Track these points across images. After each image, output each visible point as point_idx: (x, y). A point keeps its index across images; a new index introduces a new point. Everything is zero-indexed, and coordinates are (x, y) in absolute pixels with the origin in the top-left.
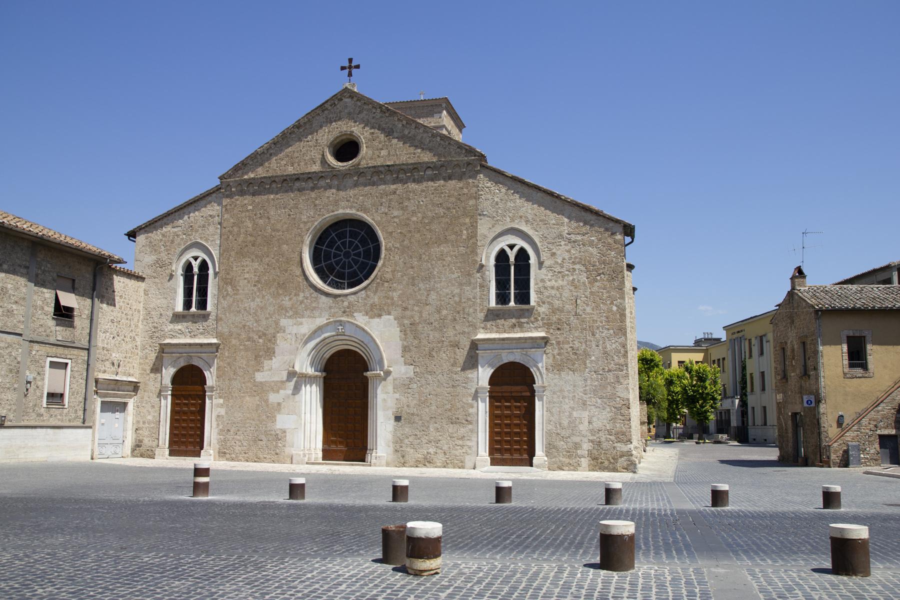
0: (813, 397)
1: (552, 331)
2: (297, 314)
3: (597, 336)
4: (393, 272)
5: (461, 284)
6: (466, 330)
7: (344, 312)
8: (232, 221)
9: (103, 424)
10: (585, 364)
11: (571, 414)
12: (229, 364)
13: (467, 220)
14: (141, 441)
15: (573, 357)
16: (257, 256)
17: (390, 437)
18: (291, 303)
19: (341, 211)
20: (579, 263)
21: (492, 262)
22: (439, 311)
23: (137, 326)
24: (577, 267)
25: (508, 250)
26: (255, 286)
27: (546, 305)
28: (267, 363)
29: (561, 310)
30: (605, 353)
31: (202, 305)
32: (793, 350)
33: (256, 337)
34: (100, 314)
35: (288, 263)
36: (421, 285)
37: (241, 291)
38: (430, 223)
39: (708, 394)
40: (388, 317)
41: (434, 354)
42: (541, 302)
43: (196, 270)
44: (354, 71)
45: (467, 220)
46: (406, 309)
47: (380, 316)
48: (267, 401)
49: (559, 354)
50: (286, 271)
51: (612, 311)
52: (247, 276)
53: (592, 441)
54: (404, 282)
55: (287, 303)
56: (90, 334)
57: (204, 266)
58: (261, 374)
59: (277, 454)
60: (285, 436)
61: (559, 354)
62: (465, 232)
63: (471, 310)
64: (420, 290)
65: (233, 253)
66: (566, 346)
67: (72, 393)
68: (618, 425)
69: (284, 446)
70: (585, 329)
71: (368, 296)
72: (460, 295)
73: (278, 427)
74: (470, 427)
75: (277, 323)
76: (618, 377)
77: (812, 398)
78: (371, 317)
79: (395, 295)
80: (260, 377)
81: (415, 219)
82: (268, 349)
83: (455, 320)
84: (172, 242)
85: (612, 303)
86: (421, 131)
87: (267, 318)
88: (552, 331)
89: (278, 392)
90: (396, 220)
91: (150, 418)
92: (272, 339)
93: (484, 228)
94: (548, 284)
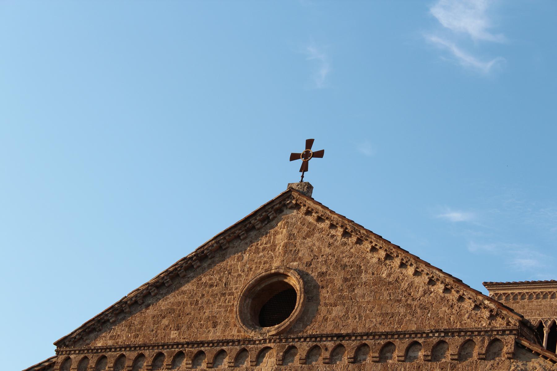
44: (313, 162)
86: (410, 271)
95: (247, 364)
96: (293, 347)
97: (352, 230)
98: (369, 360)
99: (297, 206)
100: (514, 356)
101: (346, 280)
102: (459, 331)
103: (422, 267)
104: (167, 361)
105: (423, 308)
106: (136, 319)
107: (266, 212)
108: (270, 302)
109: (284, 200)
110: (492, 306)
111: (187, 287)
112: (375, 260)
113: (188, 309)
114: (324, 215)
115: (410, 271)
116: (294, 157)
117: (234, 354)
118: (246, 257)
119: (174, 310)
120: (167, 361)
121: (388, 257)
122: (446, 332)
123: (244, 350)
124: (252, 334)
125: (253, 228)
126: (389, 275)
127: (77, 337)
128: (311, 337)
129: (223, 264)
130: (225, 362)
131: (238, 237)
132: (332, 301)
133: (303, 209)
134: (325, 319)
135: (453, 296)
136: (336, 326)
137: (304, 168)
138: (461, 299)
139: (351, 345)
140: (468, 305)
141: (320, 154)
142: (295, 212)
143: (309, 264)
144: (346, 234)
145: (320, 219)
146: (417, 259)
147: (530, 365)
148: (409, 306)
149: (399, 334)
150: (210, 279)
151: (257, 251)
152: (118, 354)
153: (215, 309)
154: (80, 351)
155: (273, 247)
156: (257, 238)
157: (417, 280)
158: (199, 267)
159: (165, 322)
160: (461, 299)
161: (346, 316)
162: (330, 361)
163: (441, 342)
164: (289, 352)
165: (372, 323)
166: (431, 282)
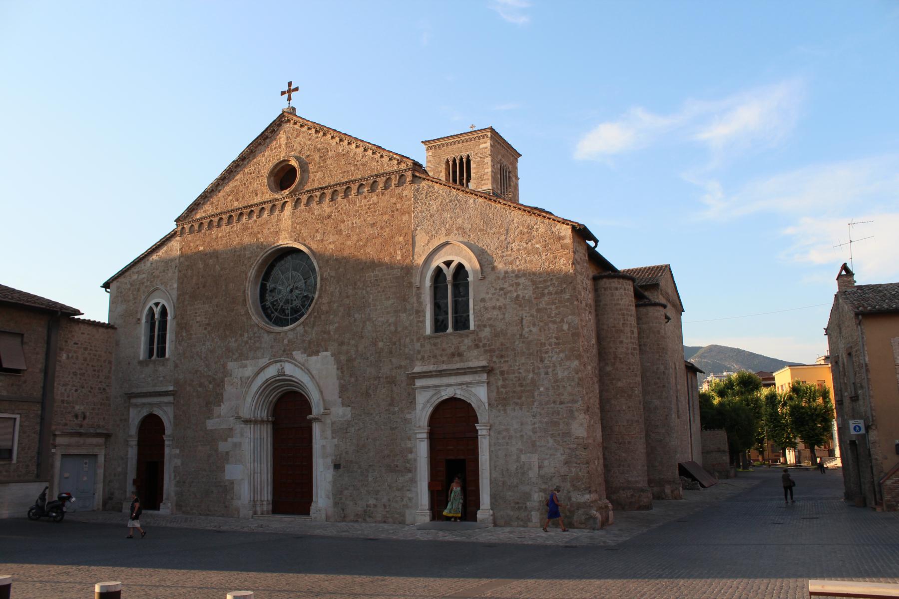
0: (862, 422)
1: (495, 359)
2: (242, 357)
3: (546, 362)
4: (329, 303)
5: (396, 312)
6: (403, 364)
7: (284, 351)
8: (186, 263)
9: (67, 478)
10: (534, 398)
11: (518, 458)
13: (401, 239)
14: (112, 494)
15: (519, 389)
17: (329, 487)
21: (428, 283)
22: (375, 344)
23: (108, 377)
24: (522, 280)
25: (443, 266)
26: (205, 329)
27: (487, 329)
28: (216, 410)
30: (556, 381)
31: (162, 352)
32: (843, 364)
33: (207, 383)
34: (58, 368)
36: (356, 316)
37: (194, 336)
38: (364, 246)
39: (817, 415)
40: (325, 353)
41: (370, 391)
42: (481, 327)
43: (156, 316)
45: (401, 239)
46: (342, 344)
47: (317, 353)
50: (232, 311)
52: (198, 319)
53: (544, 491)
54: (340, 314)
55: (233, 345)
56: (44, 388)
57: (164, 312)
58: (211, 421)
59: (226, 507)
60: (233, 488)
61: (504, 386)
62: (399, 252)
63: (408, 340)
64: (355, 320)
65: (187, 297)
66: (512, 376)
67: (21, 448)
68: (574, 470)
69: (232, 499)
70: (531, 354)
71: (305, 331)
73: (227, 478)
74: (410, 475)
75: (224, 366)
76: (571, 411)
77: (861, 423)
78: (309, 355)
79: (332, 328)
80: (211, 424)
81: (349, 243)
83: (391, 352)
84: (139, 290)
86: (354, 146)
87: (216, 363)
88: (495, 359)
89: (226, 440)
90: (331, 246)
91: (119, 470)
92: (220, 384)
94: (488, 304)
95: (277, 212)
96: (299, 199)
97: (319, 129)
98: (339, 198)
99: (289, 121)
100: (412, 182)
101: (321, 157)
102: (383, 174)
103: (359, 143)
104: (235, 219)
105: (363, 165)
106: (215, 199)
108: (284, 176)
110: (398, 157)
111: (238, 177)
112: (334, 143)
113: (241, 188)
114: (304, 123)
115: (354, 146)
116: (283, 93)
117: (269, 208)
118: (266, 154)
120: (235, 219)
121: (341, 140)
122: (376, 176)
123: (274, 205)
124: (277, 196)
128: (307, 191)
129: (255, 161)
130: (266, 214)
133: (292, 122)
134: (314, 180)
135: (378, 156)
136: (320, 183)
137: (289, 99)
138: (382, 156)
139: (329, 192)
140: (386, 159)
141: (296, 89)
142: (288, 125)
143: (300, 152)
144: (317, 132)
145: (302, 126)
146: (356, 139)
147: (421, 185)
149: (352, 181)
151: (272, 150)
152: (208, 220)
153: (255, 186)
155: (280, 147)
156: (270, 143)
157: (358, 150)
159: (230, 198)
160: (382, 156)
161: (324, 177)
162: (320, 202)
163: (375, 182)
164: (298, 202)
165: (339, 178)
166: (365, 150)
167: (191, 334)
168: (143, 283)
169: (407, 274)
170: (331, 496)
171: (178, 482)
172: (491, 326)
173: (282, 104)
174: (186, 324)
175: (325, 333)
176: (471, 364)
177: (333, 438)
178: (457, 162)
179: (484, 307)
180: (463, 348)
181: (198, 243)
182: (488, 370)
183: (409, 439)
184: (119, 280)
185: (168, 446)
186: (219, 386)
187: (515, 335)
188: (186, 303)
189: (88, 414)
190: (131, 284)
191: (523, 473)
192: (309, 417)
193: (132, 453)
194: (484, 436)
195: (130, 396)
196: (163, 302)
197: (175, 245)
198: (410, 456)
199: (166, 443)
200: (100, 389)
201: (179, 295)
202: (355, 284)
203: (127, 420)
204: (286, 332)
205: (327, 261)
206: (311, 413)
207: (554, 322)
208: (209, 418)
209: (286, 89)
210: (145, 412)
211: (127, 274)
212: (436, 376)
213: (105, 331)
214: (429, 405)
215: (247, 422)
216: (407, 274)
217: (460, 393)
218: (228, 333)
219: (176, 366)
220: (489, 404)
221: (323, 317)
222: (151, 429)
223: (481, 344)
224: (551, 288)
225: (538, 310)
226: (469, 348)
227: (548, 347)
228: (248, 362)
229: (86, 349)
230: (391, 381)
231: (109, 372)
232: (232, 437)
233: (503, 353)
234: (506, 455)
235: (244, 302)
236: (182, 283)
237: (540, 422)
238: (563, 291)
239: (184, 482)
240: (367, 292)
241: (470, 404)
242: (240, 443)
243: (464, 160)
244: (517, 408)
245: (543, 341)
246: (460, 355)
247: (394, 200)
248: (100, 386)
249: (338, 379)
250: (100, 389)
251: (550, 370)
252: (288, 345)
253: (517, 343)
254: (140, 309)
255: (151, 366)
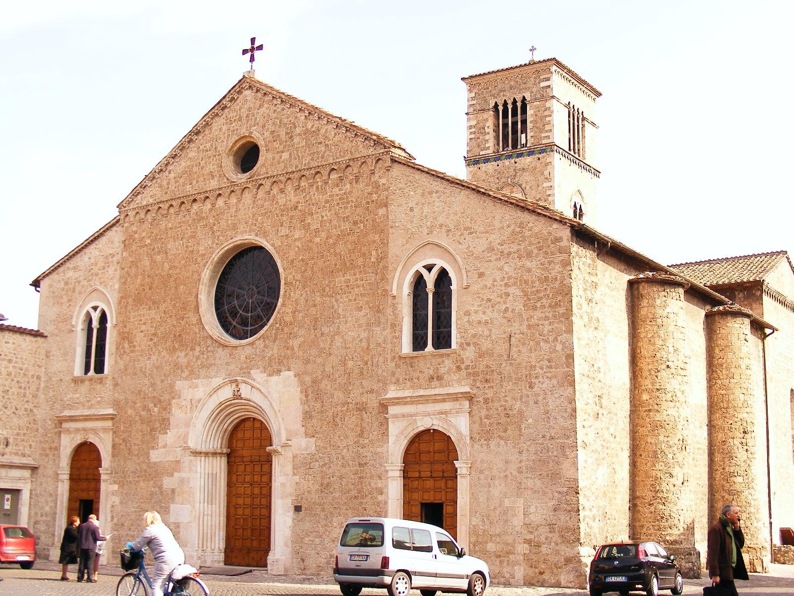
1: (478, 384)
2: (192, 374)
5: (368, 324)
6: (375, 387)
8: (130, 259)
10: (520, 430)
12: (124, 440)
13: (377, 237)
15: (504, 420)
16: (154, 303)
17: (288, 532)
18: (186, 360)
19: (239, 237)
20: (515, 284)
22: (344, 363)
23: (35, 396)
24: (511, 290)
25: (425, 273)
26: (151, 340)
27: (472, 348)
28: (162, 439)
29: (489, 353)
31: (100, 369)
35: (185, 308)
37: (137, 348)
38: (334, 244)
41: (337, 420)
46: (308, 362)
47: (279, 372)
48: (160, 487)
49: (487, 417)
50: (183, 318)
51: (555, 351)
53: (529, 542)
55: (183, 360)
57: (103, 318)
58: (155, 452)
61: (487, 417)
62: (374, 253)
63: (381, 359)
64: (322, 334)
65: (130, 300)
66: (496, 404)
68: (562, 518)
71: (266, 346)
72: (368, 340)
75: (172, 386)
78: (270, 375)
79: (295, 343)
80: (155, 456)
81: (317, 240)
82: (164, 420)
83: (362, 373)
84: (74, 291)
85: (556, 339)
88: (478, 384)
89: (172, 475)
90: (298, 244)
91: (47, 509)
92: (166, 408)
93: (396, 246)
94: (474, 317)
101: (287, 133)
107: (232, 94)
109: (242, 85)
117: (227, 194)
119: (187, 172)
125: (226, 107)
126: (312, 126)
127: (130, 200)
131: (217, 114)
132: (281, 149)
137: (252, 59)
148: (327, 145)
150: (205, 147)
154: (133, 209)
158: (196, 139)
159: (181, 181)
167: (134, 346)
168: (79, 282)
169: (382, 280)
170: (290, 545)
171: (116, 525)
172: (475, 344)
173: (242, 65)
174: (128, 333)
175: (288, 348)
176: (451, 390)
177: (294, 474)
178: (510, 107)
179: (469, 322)
180: (442, 370)
181: (144, 234)
182: (470, 398)
183: (380, 478)
184: (51, 276)
185: (106, 481)
186: (165, 409)
187: (501, 356)
188: (129, 308)
189: (11, 441)
190: (66, 283)
191: (506, 521)
192: (269, 448)
193: (63, 489)
194: (463, 476)
195: (61, 421)
196: (102, 306)
197: (116, 235)
198: (380, 498)
199: (103, 477)
200: (26, 410)
201: (122, 298)
202: (324, 290)
203: (57, 449)
204: (243, 346)
205: (292, 261)
206: (271, 445)
207: (547, 341)
208: (153, 448)
209: (248, 46)
210: (79, 440)
211: (61, 269)
212: (412, 403)
213: (33, 339)
214: (403, 437)
215: (196, 453)
216: (382, 280)
217: (436, 424)
218: (177, 346)
219: (116, 385)
220: (471, 438)
221: (286, 329)
222: (85, 459)
223: (463, 366)
224: (544, 301)
225: (529, 327)
226: (450, 369)
227: (538, 370)
228: (199, 381)
229: (10, 361)
230: (361, 408)
231: (38, 389)
232: (179, 471)
233: (488, 377)
234: (488, 499)
235: (197, 308)
236: (125, 283)
237: (528, 460)
238: (557, 305)
239: (123, 525)
240: (337, 301)
241: (449, 437)
242: (188, 479)
243: (519, 104)
244: (502, 442)
245: (533, 363)
246: (440, 378)
247: (370, 189)
248: (26, 406)
249: (301, 403)
250: (26, 410)
251: (540, 398)
252: (245, 363)
253: (504, 365)
254: (75, 314)
255: (87, 383)
